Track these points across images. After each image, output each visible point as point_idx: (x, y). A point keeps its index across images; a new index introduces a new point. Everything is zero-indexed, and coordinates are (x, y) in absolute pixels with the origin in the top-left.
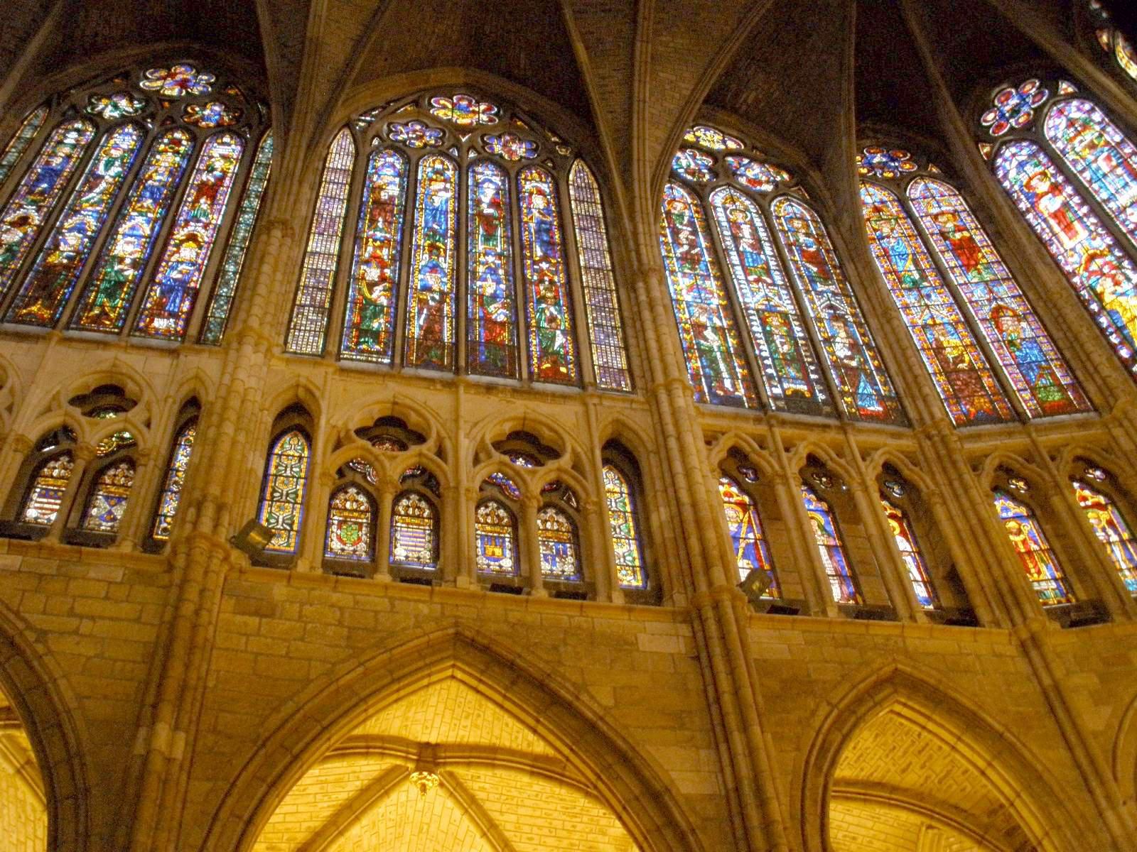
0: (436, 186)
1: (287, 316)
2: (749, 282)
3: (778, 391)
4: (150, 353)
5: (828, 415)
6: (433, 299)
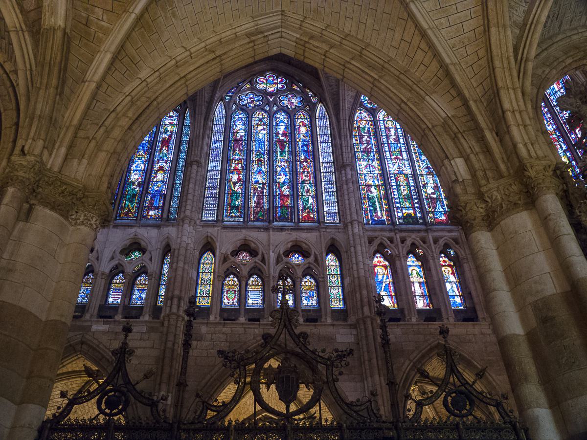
0: (261, 127)
1: (202, 204)
2: (391, 159)
3: (400, 215)
4: (149, 228)
5: (421, 224)
6: (259, 187)
